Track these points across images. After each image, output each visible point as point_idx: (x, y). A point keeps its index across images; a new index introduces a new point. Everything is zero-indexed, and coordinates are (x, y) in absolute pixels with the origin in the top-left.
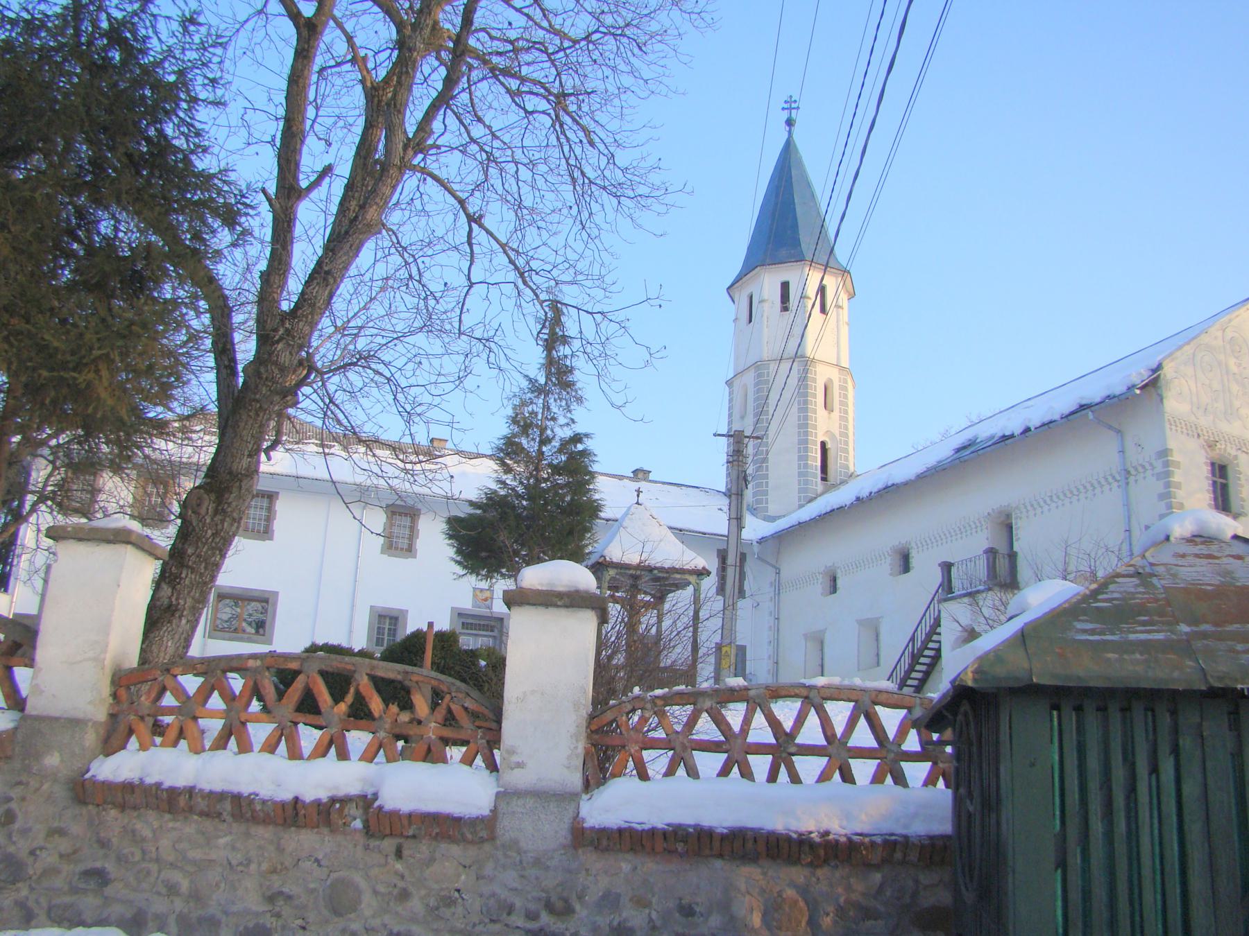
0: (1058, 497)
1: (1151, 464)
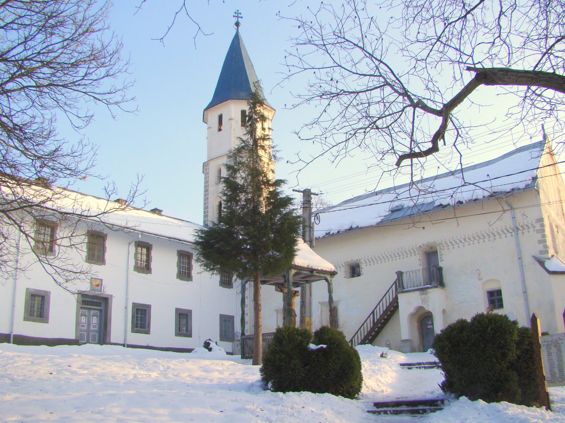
0: (470, 239)
1: (532, 225)
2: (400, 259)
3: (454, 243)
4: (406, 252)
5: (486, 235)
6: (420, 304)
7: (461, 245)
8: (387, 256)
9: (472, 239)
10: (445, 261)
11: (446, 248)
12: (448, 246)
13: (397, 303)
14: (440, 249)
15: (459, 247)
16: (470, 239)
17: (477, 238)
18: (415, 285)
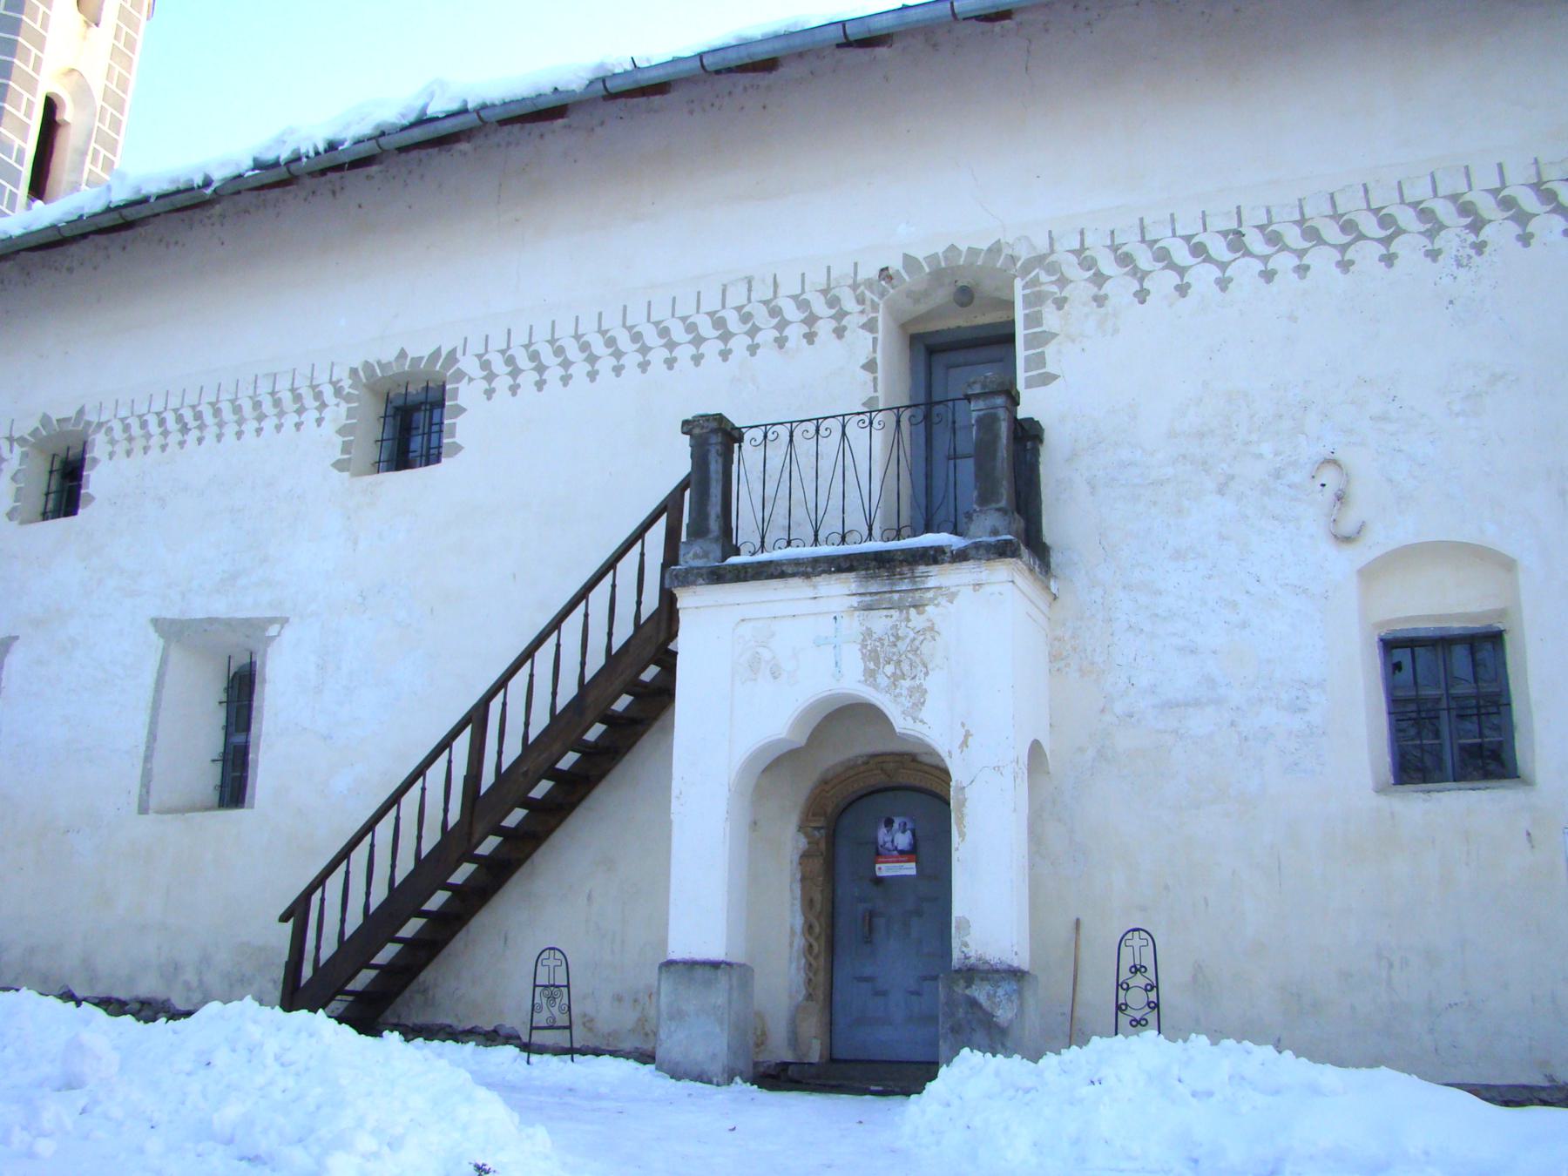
0: (1274, 239)
2: (725, 355)
3: (1144, 260)
4: (775, 312)
5: (1406, 218)
6: (852, 682)
7: (1203, 276)
8: (636, 337)
9: (1293, 236)
10: (1065, 386)
11: (1080, 288)
12: (1099, 279)
13: (668, 662)
14: (1035, 300)
15: (1183, 290)
16: (1274, 239)
17: (1332, 233)
18: (831, 525)
